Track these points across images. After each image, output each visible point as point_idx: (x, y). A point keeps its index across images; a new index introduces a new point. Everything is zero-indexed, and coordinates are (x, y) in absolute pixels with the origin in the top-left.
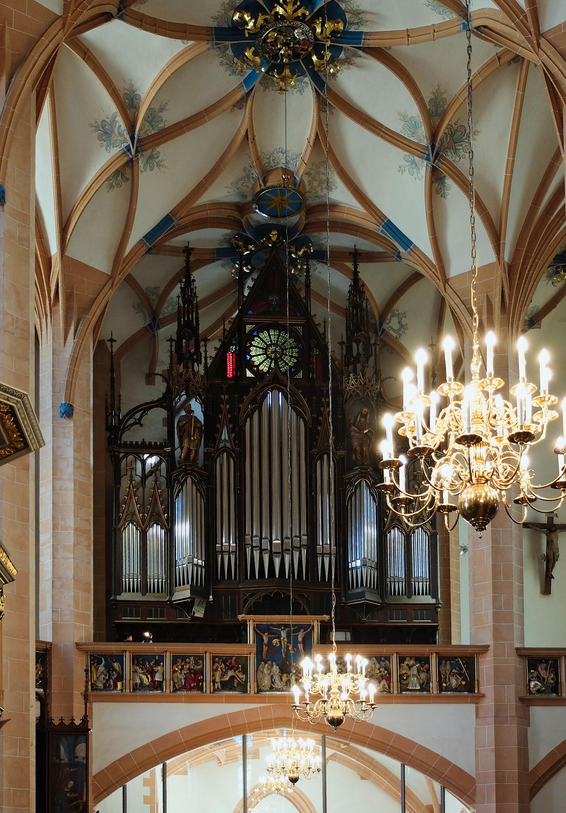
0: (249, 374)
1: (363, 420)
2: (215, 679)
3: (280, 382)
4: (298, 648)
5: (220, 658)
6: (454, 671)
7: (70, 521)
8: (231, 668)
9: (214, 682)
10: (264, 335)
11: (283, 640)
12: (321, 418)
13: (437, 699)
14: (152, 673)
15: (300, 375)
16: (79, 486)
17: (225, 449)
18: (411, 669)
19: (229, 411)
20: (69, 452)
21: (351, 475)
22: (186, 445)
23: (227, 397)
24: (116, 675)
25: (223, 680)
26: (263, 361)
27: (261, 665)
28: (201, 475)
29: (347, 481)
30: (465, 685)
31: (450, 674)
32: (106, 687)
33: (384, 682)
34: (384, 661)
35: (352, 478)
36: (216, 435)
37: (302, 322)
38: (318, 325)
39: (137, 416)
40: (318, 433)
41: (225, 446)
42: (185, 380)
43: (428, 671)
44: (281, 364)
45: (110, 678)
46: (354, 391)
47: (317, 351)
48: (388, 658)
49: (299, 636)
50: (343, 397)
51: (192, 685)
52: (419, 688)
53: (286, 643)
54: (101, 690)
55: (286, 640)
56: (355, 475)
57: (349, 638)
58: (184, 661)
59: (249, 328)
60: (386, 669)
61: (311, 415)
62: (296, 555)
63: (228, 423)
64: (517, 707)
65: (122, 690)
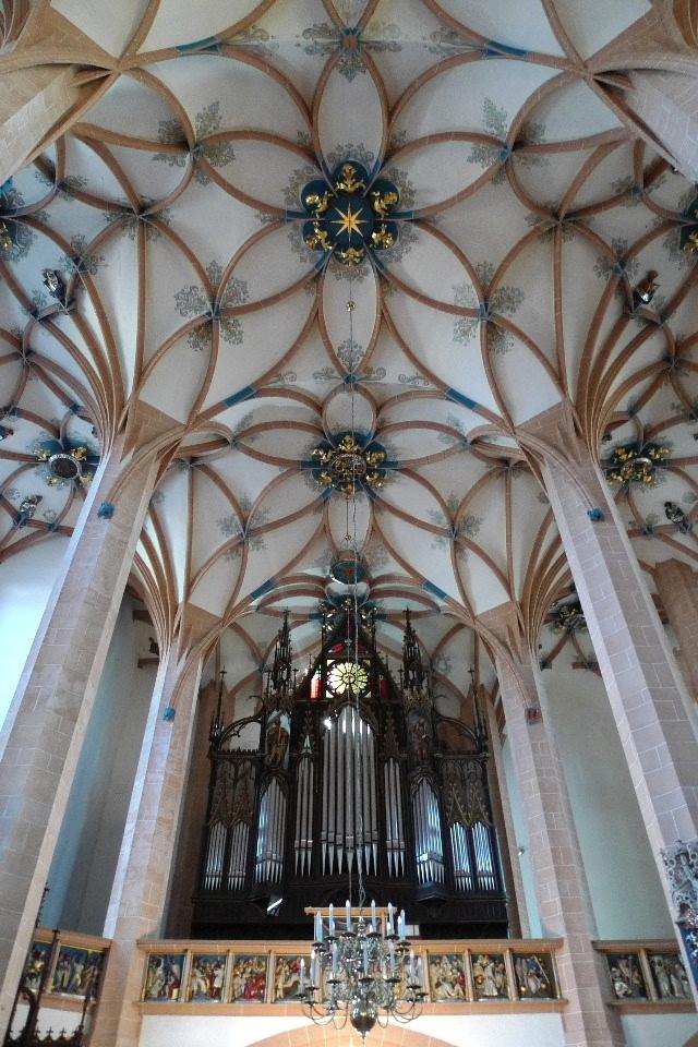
5: (285, 958)
6: (531, 971)
7: (155, 811)
9: (276, 989)
10: (341, 666)
13: (518, 1010)
14: (212, 978)
15: (369, 695)
16: (170, 779)
17: (307, 755)
20: (165, 749)
21: (414, 773)
22: (273, 751)
24: (173, 980)
25: (286, 986)
30: (546, 990)
32: (161, 995)
33: (458, 987)
39: (236, 729)
43: (504, 971)
44: (353, 686)
48: (459, 956)
51: (252, 993)
52: (496, 993)
54: (155, 999)
57: (417, 933)
59: (329, 662)
62: (367, 849)
64: (607, 1016)
65: (177, 999)
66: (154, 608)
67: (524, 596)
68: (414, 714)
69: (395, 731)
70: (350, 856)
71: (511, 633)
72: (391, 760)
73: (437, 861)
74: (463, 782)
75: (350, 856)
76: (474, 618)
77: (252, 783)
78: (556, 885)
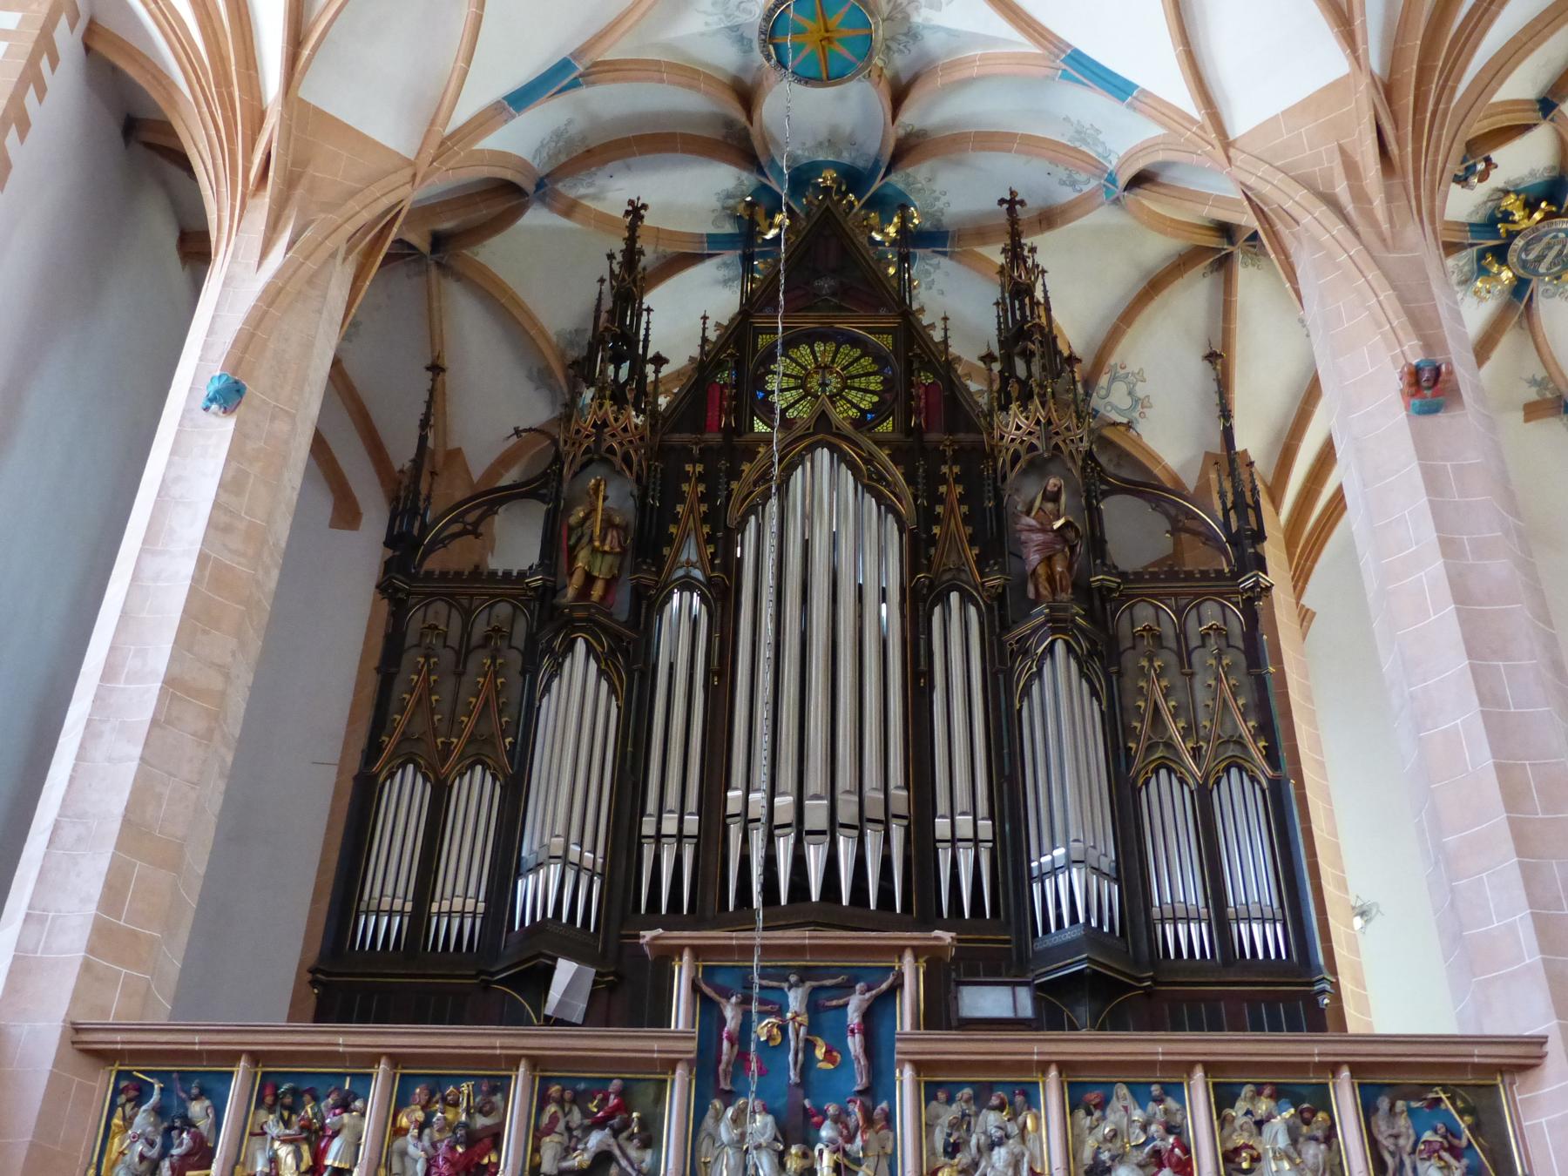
0: (759, 427)
1: (1050, 506)
2: (540, 1165)
3: (834, 429)
4: (845, 1051)
6: (1428, 1136)
8: (600, 1124)
11: (793, 1019)
12: (939, 509)
18: (1266, 1128)
19: (703, 498)
21: (1024, 629)
23: (700, 468)
25: (565, 1164)
26: (797, 402)
27: (711, 1112)
28: (616, 637)
29: (1015, 647)
31: (1413, 1152)
34: (1159, 1101)
35: (1029, 636)
36: (666, 551)
37: (893, 323)
38: (929, 326)
39: (471, 517)
40: (932, 540)
41: (687, 576)
42: (595, 425)
43: (1330, 1136)
45: (165, 1153)
46: (1022, 442)
47: (927, 378)
49: (851, 1009)
50: (995, 460)
53: (802, 1031)
55: (803, 1019)
56: (1035, 630)
57: (1026, 1009)
58: (438, 1096)
60: (1169, 1129)
61: (915, 500)
63: (698, 524)
66: (203, 145)
67: (1395, 57)
68: (1025, 472)
69: (966, 520)
70: (815, 859)
71: (1351, 169)
72: (954, 597)
73: (1097, 870)
74: (1184, 657)
75: (815, 859)
76: (1227, 144)
77: (515, 659)
78: (1516, 874)
